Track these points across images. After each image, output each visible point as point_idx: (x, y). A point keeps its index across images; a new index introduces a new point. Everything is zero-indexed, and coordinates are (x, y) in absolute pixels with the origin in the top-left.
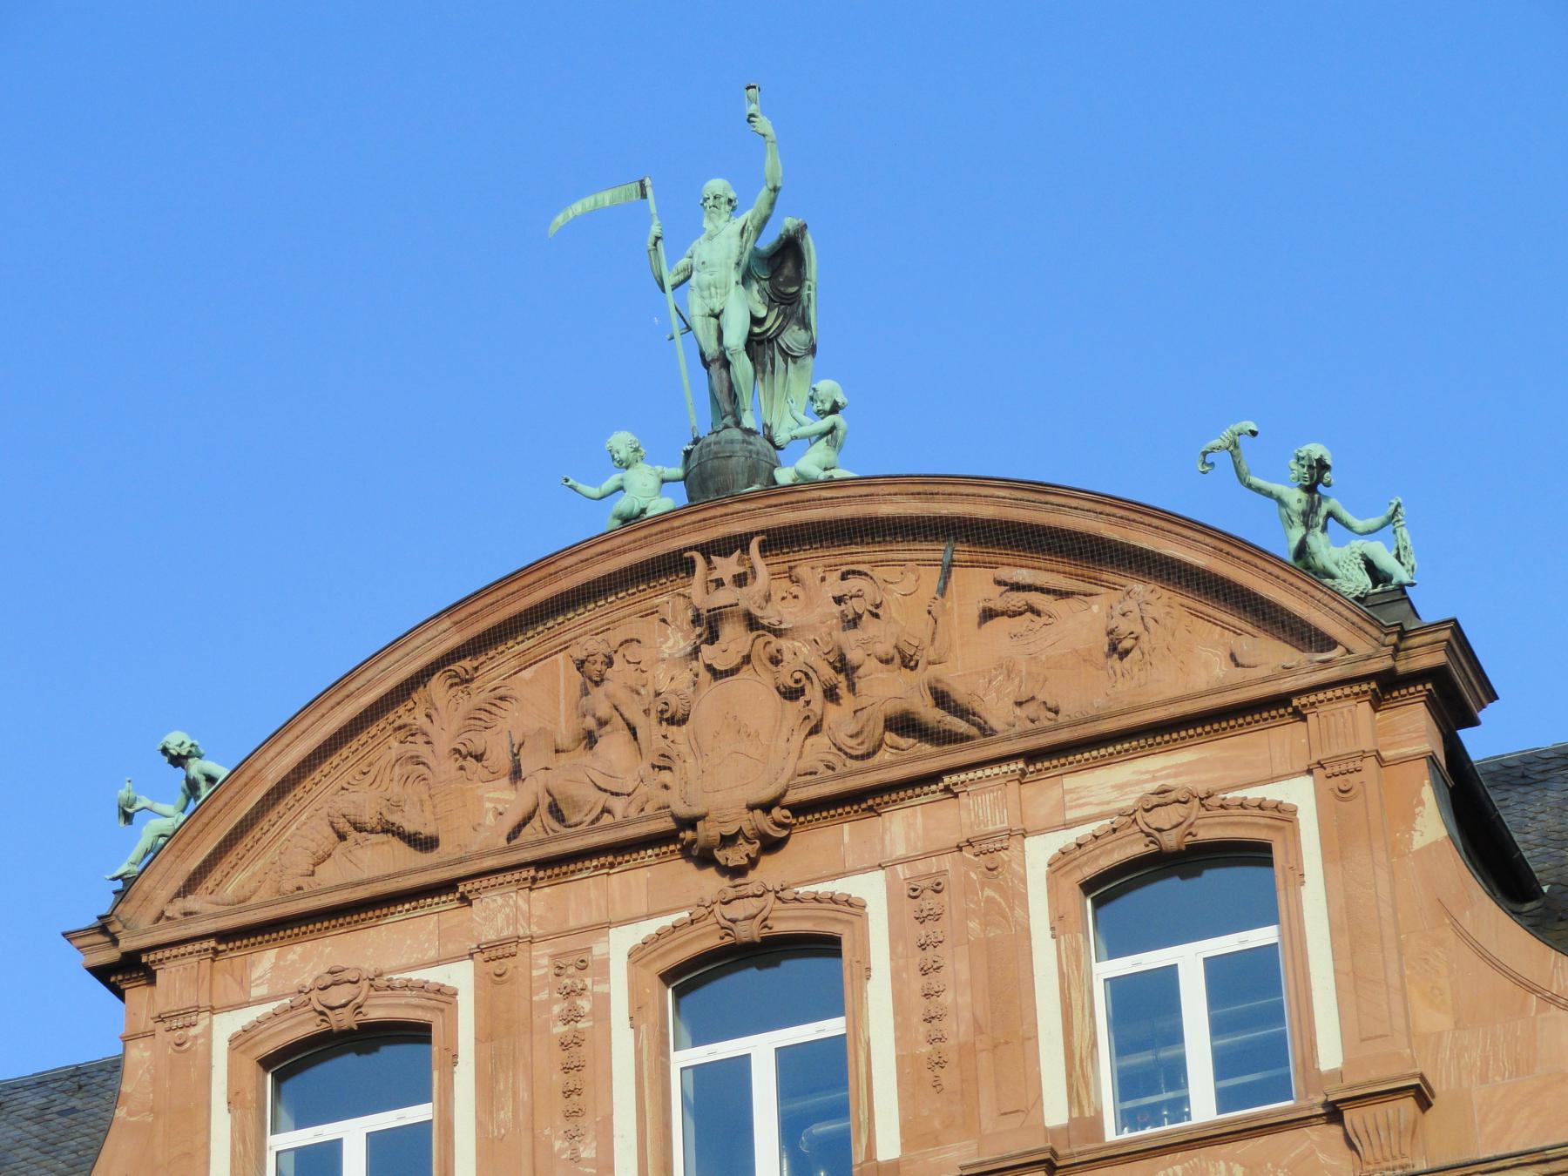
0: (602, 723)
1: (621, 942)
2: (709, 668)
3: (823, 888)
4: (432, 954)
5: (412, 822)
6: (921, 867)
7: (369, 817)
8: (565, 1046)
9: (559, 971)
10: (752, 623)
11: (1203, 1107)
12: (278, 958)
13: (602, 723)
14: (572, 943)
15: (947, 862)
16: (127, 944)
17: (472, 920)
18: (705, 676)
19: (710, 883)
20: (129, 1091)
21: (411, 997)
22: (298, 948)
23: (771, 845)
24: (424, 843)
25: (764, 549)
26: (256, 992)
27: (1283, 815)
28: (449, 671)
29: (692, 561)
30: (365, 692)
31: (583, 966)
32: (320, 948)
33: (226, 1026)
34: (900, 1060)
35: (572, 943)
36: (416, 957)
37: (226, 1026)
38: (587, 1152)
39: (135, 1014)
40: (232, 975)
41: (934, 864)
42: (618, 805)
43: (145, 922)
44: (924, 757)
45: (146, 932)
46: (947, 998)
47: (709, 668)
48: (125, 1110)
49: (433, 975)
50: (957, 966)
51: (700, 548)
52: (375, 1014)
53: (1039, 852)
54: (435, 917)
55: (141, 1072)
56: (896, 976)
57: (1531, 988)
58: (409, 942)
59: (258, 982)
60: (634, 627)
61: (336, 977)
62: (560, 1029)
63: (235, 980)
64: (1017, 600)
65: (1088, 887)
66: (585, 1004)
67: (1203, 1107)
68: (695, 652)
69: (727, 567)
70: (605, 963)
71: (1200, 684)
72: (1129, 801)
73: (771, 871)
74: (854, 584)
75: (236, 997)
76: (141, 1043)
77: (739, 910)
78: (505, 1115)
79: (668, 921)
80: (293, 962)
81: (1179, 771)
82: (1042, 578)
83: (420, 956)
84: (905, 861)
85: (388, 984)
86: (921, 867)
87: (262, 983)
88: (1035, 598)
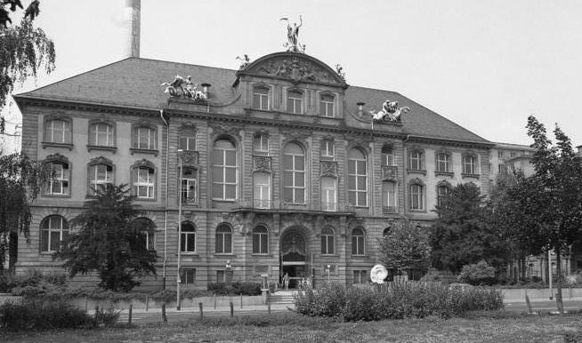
44: (309, 81)
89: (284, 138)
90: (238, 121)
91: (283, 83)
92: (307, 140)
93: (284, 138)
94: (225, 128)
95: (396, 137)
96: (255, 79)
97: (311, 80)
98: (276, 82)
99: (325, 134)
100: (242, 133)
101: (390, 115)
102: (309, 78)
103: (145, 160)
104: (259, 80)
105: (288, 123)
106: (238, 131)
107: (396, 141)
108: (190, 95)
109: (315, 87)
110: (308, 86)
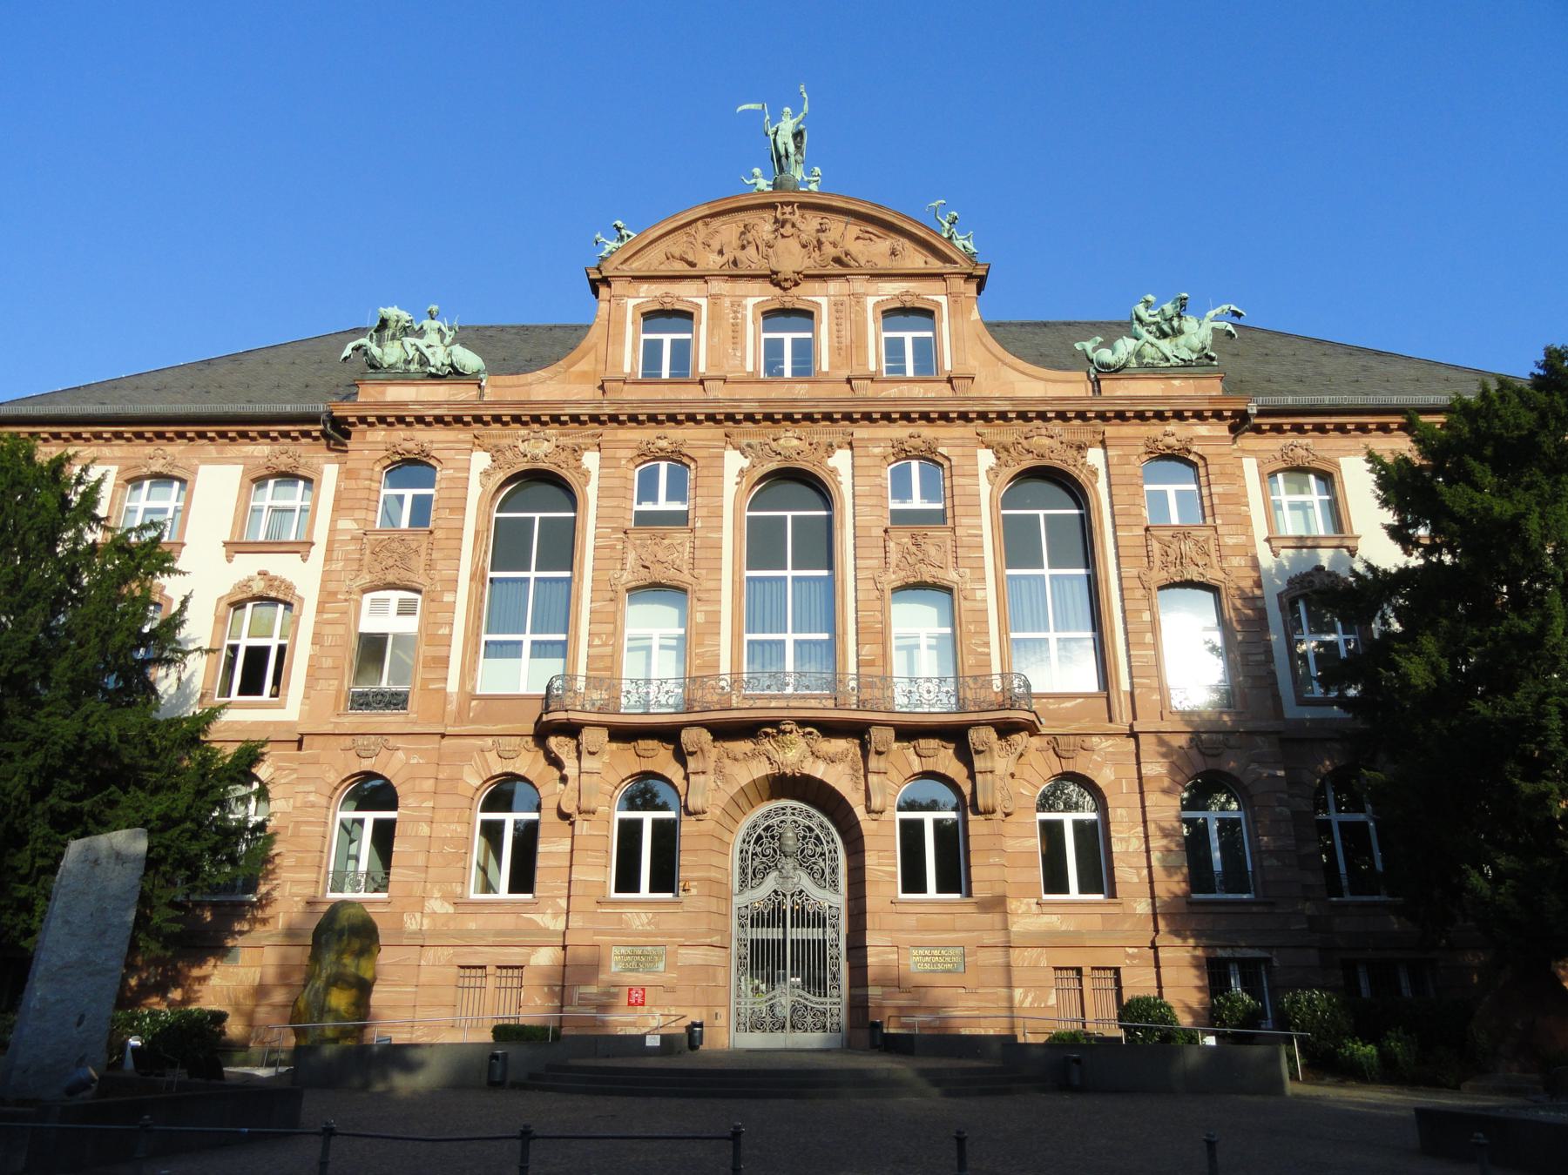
0: (749, 243)
1: (750, 302)
2: (782, 235)
3: (809, 298)
5: (691, 258)
6: (838, 298)
7: (677, 254)
8: (733, 325)
9: (732, 305)
10: (793, 225)
11: (910, 372)
13: (749, 243)
14: (736, 299)
15: (845, 298)
16: (604, 274)
18: (779, 236)
19: (777, 291)
21: (689, 304)
23: (796, 284)
24: (692, 265)
25: (798, 207)
26: (641, 295)
27: (939, 304)
29: (777, 207)
31: (739, 305)
33: (631, 303)
34: (829, 346)
35: (736, 299)
37: (631, 303)
38: (739, 354)
41: (841, 298)
42: (753, 266)
43: (611, 269)
44: (838, 270)
46: (843, 333)
47: (782, 235)
49: (695, 300)
50: (846, 326)
51: (780, 203)
52: (677, 307)
53: (870, 302)
56: (829, 324)
57: (999, 360)
60: (756, 221)
61: (667, 295)
62: (732, 321)
64: (867, 235)
65: (883, 312)
66: (740, 316)
67: (910, 372)
68: (776, 230)
69: (788, 209)
70: (746, 306)
71: (916, 266)
72: (897, 292)
73: (794, 291)
74: (825, 220)
75: (635, 295)
77: (784, 299)
78: (716, 340)
79: (765, 298)
81: (911, 287)
82: (875, 232)
84: (834, 296)
86: (838, 298)
88: (872, 236)
89: (746, 463)
90: (575, 418)
91: (742, 287)
92: (831, 462)
93: (746, 463)
94: (540, 448)
95: (1199, 416)
96: (644, 288)
97: (842, 266)
98: (717, 286)
99: (900, 431)
100: (591, 460)
101: (1166, 345)
102: (837, 260)
103: (263, 574)
104: (658, 289)
105: (749, 408)
106: (576, 451)
107: (1202, 430)
108: (424, 361)
109: (859, 285)
110: (833, 287)
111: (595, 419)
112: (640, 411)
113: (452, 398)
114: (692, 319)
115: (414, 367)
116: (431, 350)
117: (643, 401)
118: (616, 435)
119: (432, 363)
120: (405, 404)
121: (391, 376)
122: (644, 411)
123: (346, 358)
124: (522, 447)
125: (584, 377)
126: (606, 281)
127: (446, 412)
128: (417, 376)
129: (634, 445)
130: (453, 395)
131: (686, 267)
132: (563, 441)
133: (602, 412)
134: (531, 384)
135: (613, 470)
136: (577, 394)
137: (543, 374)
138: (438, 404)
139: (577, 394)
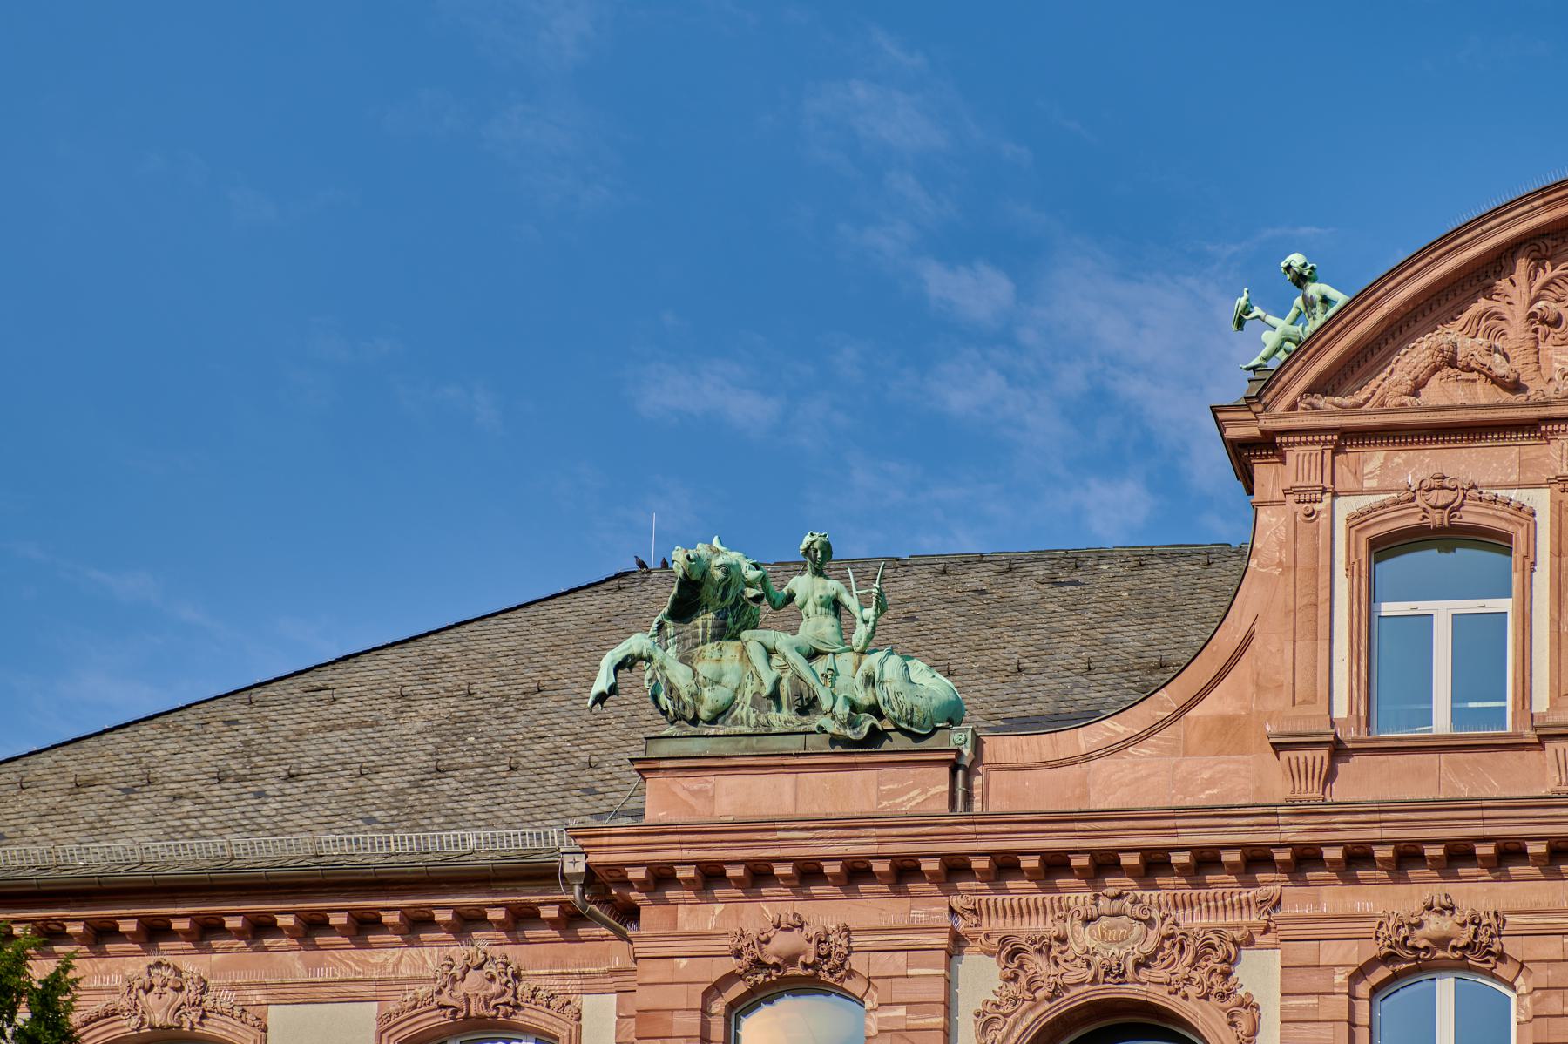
4: (1514, 478)
12: (1386, 459)
17: (1548, 456)
20: (1259, 547)
22: (1403, 455)
24: (1516, 387)
26: (1368, 484)
28: (1534, 244)
30: (1467, 249)
32: (1421, 457)
33: (1346, 507)
36: (1500, 479)
37: (1346, 507)
39: (1263, 485)
40: (1348, 467)
45: (1279, 417)
48: (1256, 561)
52: (1468, 517)
54: (1517, 449)
55: (1268, 533)
58: (1495, 465)
59: (1370, 476)
63: (1350, 471)
76: (1269, 510)
80: (1398, 465)
83: (1503, 478)
85: (1479, 495)
87: (1372, 478)
96: (1374, 460)
111: (1256, 860)
112: (1376, 835)
113: (887, 807)
114: (1508, 551)
115: (782, 718)
116: (821, 665)
117: (1383, 807)
118: (1317, 904)
119: (826, 704)
120: (767, 826)
121: (725, 747)
122: (1387, 834)
123: (601, 698)
124: (1083, 938)
125: (1228, 732)
126: (1270, 445)
127: (873, 849)
128: (793, 744)
129: (1369, 928)
130: (893, 794)
131: (1484, 393)
132: (1191, 921)
133: (1274, 838)
134: (1088, 758)
135: (1313, 1000)
136: (1211, 783)
137: (1120, 728)
138: (852, 825)
139: (1211, 783)
